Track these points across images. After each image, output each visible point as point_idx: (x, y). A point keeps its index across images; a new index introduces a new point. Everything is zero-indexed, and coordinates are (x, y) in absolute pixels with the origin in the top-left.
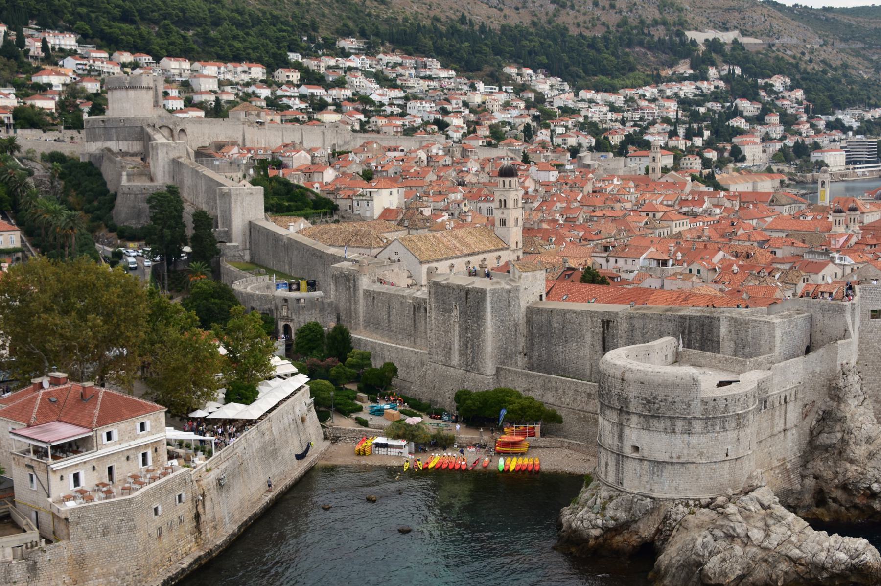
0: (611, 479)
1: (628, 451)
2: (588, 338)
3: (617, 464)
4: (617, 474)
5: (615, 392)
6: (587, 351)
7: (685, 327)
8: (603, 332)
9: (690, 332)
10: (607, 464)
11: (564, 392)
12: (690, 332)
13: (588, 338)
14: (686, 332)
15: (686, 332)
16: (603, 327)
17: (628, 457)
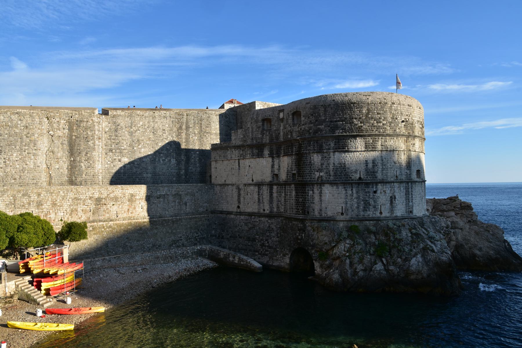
0: (400, 211)
1: (414, 176)
2: (44, 144)
3: (407, 193)
4: (407, 205)
5: (400, 118)
6: (41, 160)
7: (182, 123)
8: (70, 137)
9: (188, 128)
10: (392, 199)
11: (54, 204)
12: (188, 128)
13: (44, 144)
14: (184, 127)
15: (184, 127)
16: (71, 129)
17: (417, 182)
